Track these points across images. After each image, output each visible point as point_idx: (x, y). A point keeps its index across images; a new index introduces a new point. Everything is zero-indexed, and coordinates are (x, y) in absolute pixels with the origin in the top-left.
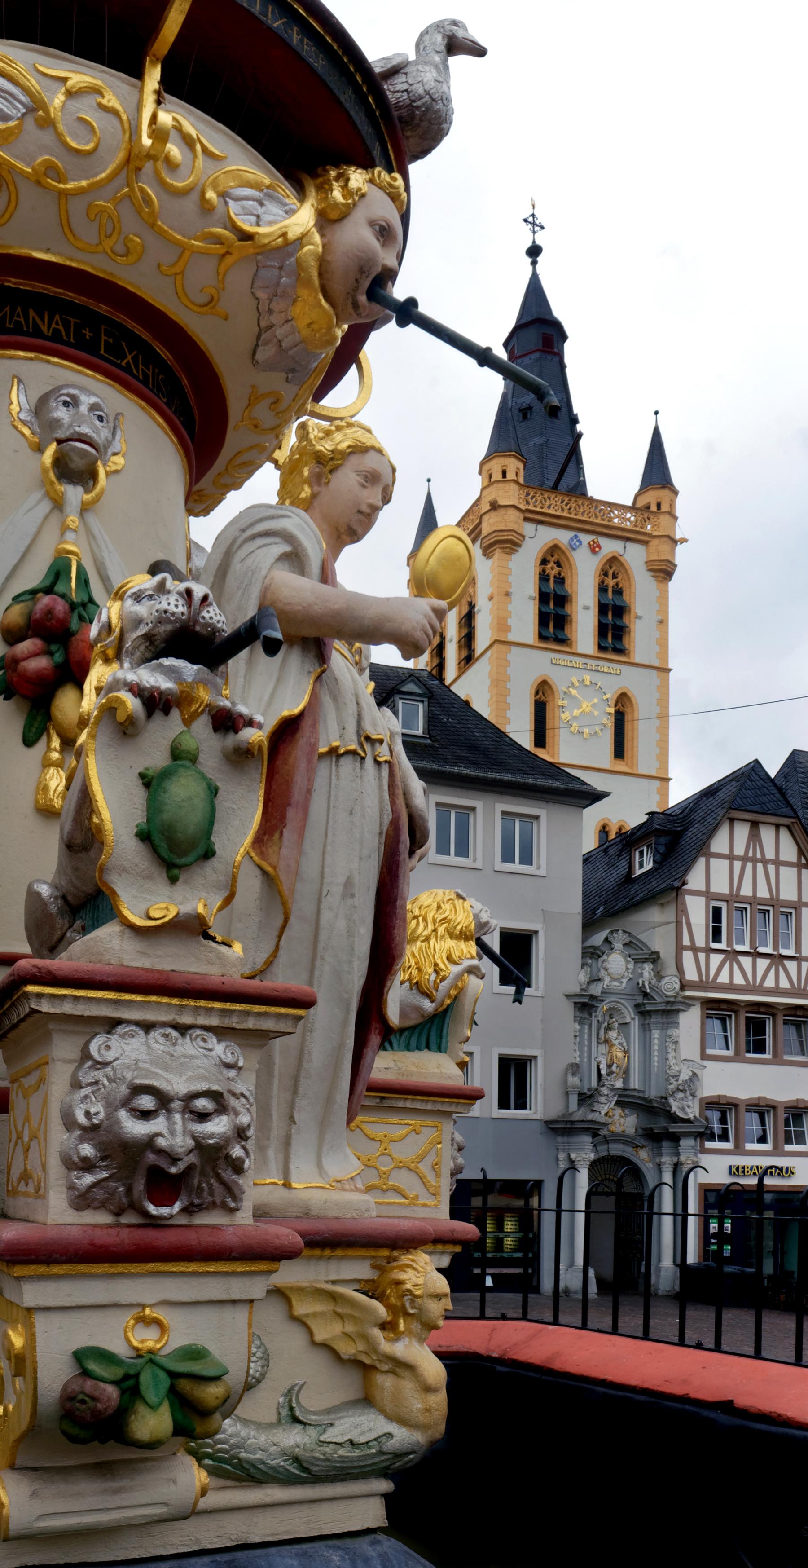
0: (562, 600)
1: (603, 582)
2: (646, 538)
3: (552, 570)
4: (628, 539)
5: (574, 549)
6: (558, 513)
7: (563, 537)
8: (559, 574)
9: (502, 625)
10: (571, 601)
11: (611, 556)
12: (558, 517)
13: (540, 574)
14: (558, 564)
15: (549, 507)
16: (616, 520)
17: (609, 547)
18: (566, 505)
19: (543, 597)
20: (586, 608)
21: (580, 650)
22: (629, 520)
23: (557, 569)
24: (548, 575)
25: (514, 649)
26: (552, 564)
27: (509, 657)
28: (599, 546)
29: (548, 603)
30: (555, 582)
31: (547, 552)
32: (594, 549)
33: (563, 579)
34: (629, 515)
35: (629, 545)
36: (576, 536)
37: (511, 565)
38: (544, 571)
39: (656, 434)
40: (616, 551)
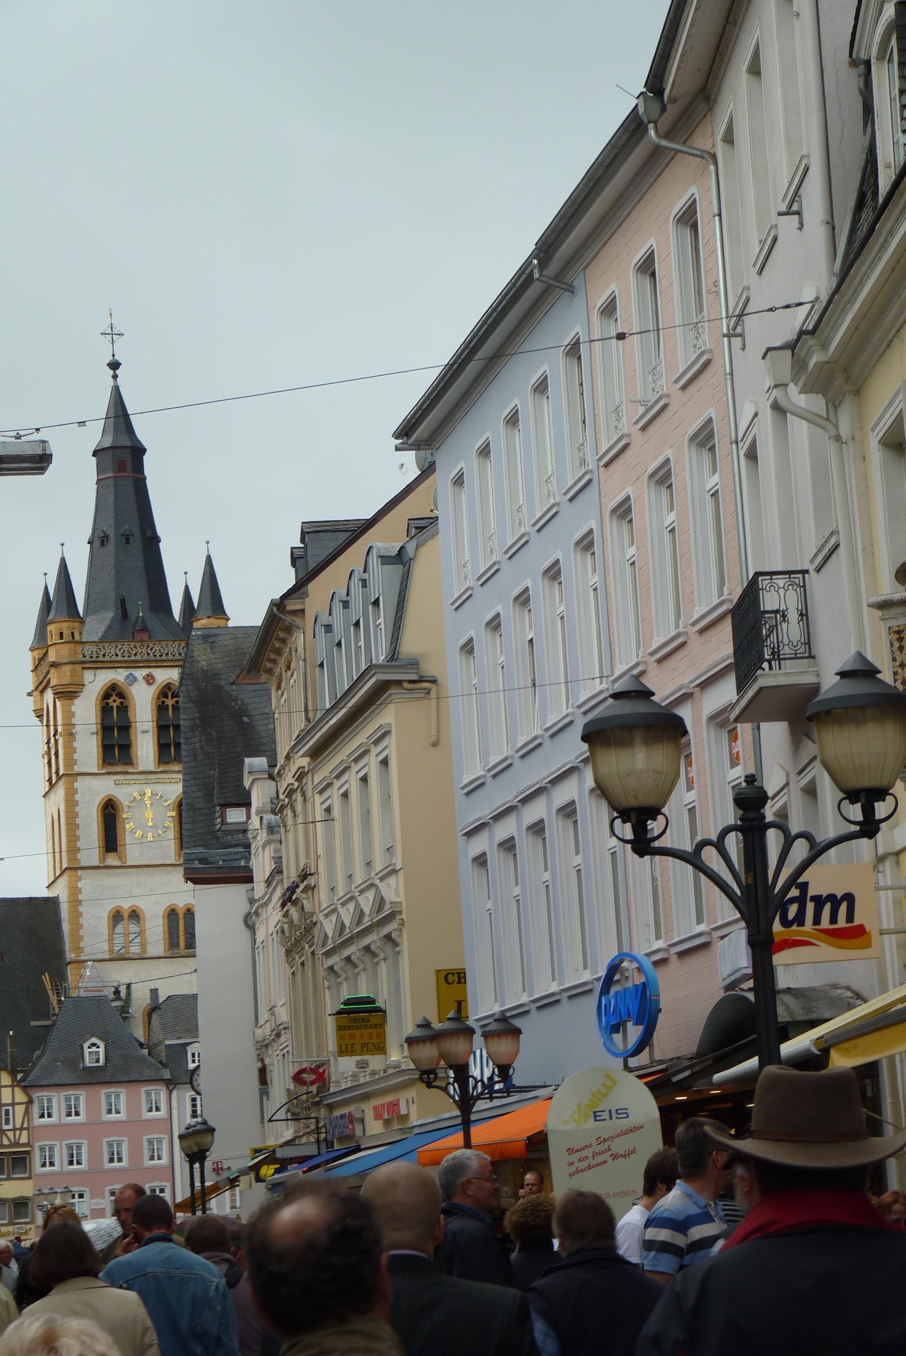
0: (126, 728)
3: (114, 702)
5: (131, 685)
6: (114, 658)
7: (119, 676)
9: (70, 761)
11: (165, 683)
13: (103, 707)
15: (104, 655)
18: (120, 650)
19: (106, 729)
20: (143, 732)
21: (141, 768)
23: (119, 701)
24: (112, 707)
26: (114, 697)
28: (153, 678)
30: (117, 711)
31: (108, 688)
32: (150, 680)
33: (126, 707)
37: (73, 709)
38: (107, 704)
39: (209, 561)
40: (170, 678)
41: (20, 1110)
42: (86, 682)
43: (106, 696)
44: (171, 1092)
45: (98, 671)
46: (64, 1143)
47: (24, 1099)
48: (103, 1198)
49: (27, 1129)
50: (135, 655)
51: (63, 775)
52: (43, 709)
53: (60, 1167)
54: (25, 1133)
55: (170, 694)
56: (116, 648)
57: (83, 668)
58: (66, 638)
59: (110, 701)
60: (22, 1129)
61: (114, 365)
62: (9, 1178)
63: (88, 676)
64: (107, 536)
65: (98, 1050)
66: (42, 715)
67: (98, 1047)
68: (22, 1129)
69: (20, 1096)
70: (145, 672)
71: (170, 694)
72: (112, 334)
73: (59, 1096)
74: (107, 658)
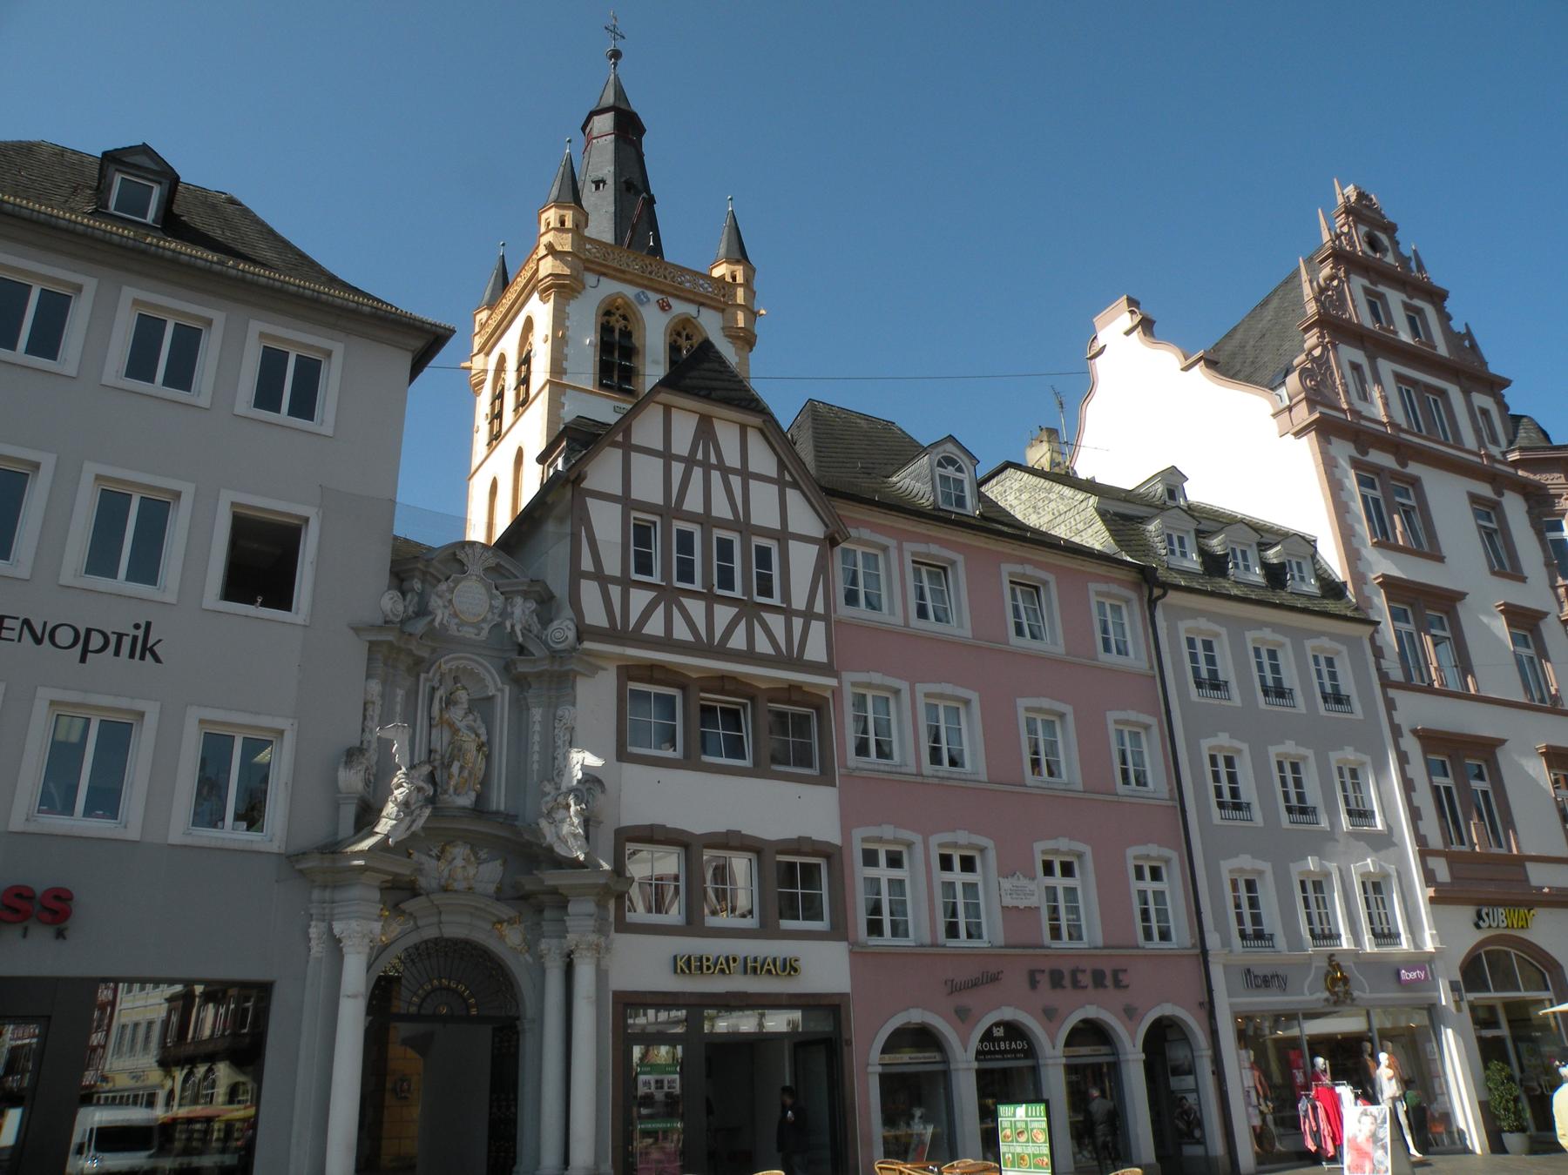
1: (675, 341)
2: (722, 306)
3: (618, 325)
4: (702, 304)
5: (642, 303)
7: (630, 291)
8: (626, 327)
10: (638, 352)
12: (623, 272)
14: (625, 318)
16: (687, 285)
17: (680, 308)
19: (605, 346)
22: (701, 286)
23: (623, 322)
25: (569, 391)
27: (563, 399)
28: (670, 307)
29: (612, 353)
32: (665, 307)
34: (701, 282)
35: (702, 309)
36: (643, 293)
37: (568, 309)
38: (608, 322)
41: (803, 558)
42: (587, 287)
43: (608, 313)
44: (1152, 603)
45: (602, 279)
46: (921, 688)
47: (816, 529)
48: (1033, 878)
49: (825, 617)
50: (651, 273)
51: (548, 381)
52: (485, 371)
53: (911, 761)
54: (818, 628)
55: (684, 334)
56: (628, 257)
57: (587, 269)
58: (569, 224)
59: (613, 319)
60: (808, 615)
61: (616, 55)
62: (758, 771)
63: (591, 279)
64: (604, 182)
65: (959, 475)
66: (483, 381)
67: (960, 470)
68: (808, 615)
69: (804, 519)
70: (659, 296)
71: (684, 334)
72: (613, 31)
73: (900, 550)
74: (615, 264)
